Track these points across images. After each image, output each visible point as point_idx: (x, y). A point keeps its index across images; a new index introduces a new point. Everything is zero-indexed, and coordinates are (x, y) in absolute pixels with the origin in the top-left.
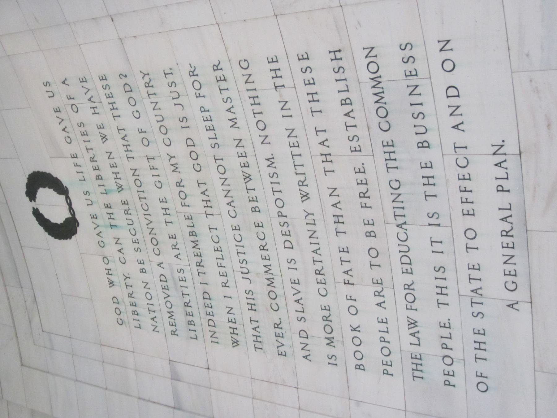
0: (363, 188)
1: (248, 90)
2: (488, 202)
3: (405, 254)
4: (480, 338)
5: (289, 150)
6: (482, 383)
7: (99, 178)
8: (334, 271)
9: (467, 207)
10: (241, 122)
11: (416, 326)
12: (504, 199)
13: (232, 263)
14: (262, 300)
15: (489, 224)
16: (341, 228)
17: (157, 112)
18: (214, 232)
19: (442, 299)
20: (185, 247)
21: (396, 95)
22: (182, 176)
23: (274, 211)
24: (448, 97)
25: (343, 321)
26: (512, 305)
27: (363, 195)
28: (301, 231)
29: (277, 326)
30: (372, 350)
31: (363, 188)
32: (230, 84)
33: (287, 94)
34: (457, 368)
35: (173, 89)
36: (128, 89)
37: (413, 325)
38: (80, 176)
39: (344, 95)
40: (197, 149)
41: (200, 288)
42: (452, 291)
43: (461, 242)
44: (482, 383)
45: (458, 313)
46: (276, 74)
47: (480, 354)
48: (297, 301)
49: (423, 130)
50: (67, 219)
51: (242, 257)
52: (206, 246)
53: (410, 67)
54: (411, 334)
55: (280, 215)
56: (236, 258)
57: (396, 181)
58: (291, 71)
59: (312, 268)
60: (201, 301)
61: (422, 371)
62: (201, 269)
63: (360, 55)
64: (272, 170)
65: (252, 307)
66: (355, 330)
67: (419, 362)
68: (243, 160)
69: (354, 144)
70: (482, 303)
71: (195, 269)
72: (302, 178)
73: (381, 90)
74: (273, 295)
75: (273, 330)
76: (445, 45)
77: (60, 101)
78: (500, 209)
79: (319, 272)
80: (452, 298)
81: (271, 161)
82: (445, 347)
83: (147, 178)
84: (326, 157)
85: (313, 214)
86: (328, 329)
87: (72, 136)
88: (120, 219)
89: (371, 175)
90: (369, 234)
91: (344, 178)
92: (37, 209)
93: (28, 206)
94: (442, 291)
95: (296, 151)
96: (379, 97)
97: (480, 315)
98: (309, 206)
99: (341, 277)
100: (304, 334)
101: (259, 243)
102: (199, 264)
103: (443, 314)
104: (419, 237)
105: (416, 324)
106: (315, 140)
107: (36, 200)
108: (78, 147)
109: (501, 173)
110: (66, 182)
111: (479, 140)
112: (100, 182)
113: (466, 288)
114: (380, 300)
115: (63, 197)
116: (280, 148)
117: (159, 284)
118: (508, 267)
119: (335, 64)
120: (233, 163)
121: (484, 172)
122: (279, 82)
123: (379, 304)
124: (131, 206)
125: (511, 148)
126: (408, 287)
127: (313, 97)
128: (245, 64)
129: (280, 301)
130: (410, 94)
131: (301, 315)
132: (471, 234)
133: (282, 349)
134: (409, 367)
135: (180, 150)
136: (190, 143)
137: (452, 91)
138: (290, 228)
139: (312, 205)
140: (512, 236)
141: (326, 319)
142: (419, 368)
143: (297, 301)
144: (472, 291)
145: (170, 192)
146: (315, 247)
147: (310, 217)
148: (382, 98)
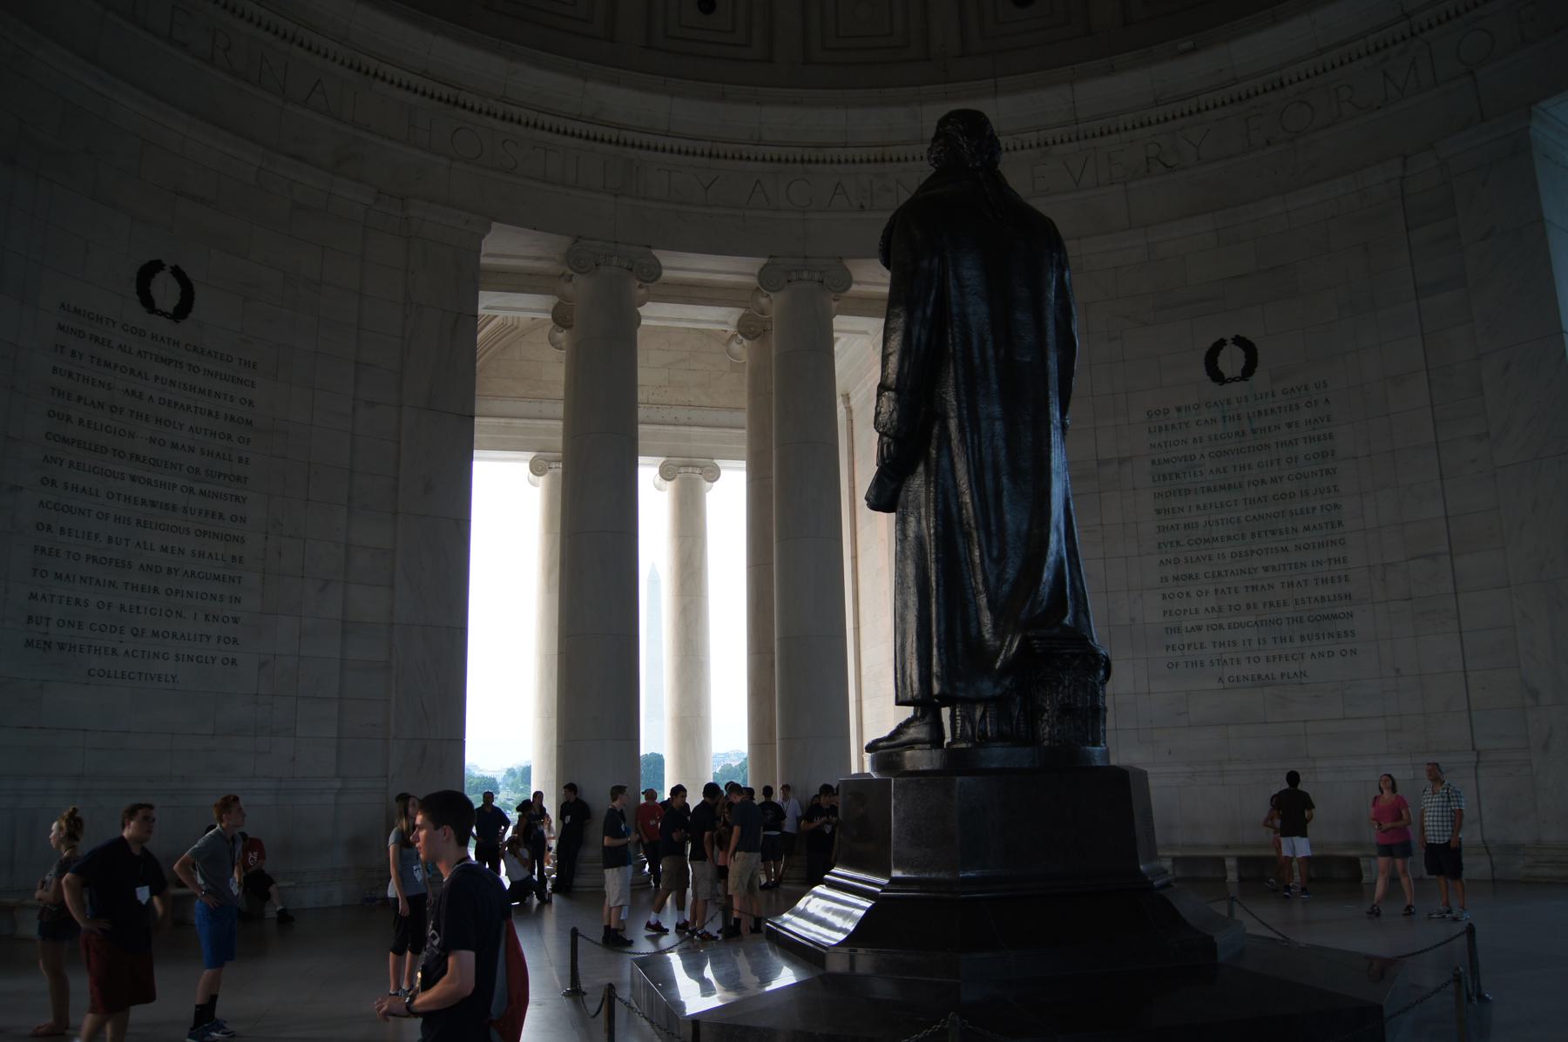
6: (1173, 665)
44: (1173, 665)
46: (1337, 561)
65: (1187, 526)
76: (1354, 652)
81: (1285, 549)
84: (1291, 584)
93: (1229, 336)
94: (1222, 644)
100: (1177, 561)
102: (1209, 489)
110: (1253, 379)
125: (1304, 680)
126: (1221, 626)
127: (1324, 581)
136: (1292, 495)
141: (1190, 577)
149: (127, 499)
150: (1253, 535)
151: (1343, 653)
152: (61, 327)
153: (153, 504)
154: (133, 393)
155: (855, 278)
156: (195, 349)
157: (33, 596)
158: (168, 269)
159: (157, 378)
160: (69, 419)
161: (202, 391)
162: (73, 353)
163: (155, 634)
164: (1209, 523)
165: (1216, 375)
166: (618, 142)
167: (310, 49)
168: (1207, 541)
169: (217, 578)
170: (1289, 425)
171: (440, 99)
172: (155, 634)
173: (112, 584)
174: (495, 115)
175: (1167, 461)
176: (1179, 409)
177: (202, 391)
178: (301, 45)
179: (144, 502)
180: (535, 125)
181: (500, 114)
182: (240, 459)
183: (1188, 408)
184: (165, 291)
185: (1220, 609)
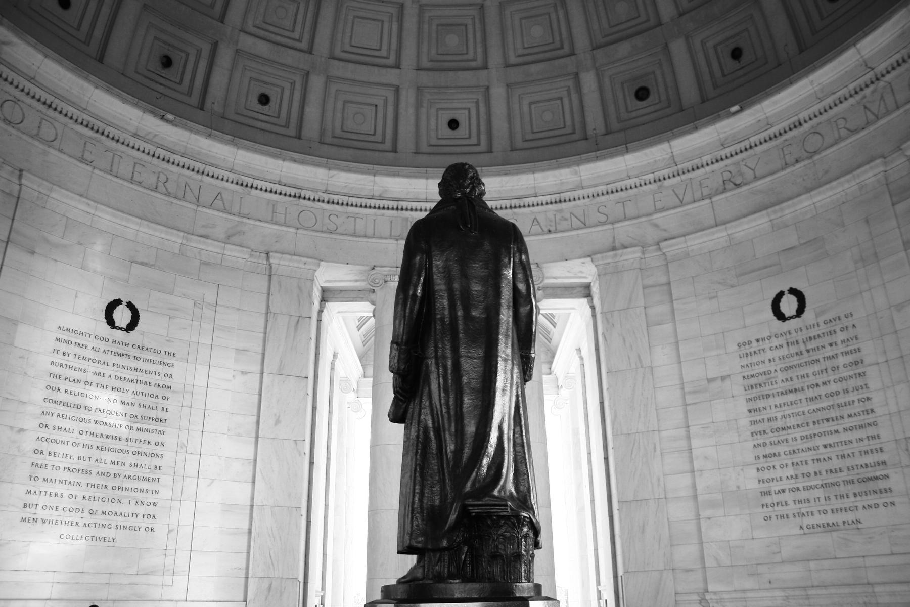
2: (839, 518)
3: (811, 487)
8: (797, 458)
12: (841, 524)
13: (788, 411)
14: (775, 425)
15: (830, 518)
20: (788, 386)
21: (871, 485)
23: (816, 432)
25: (776, 462)
27: (831, 471)
28: (810, 444)
29: (764, 432)
30: (767, 475)
32: (866, 417)
33: (866, 441)
34: (771, 509)
36: (856, 363)
41: (771, 392)
42: (801, 506)
43: (821, 508)
45: (792, 508)
46: (873, 437)
50: (783, 315)
52: (791, 397)
55: (815, 435)
56: (790, 412)
59: (795, 448)
65: (769, 420)
71: (779, 390)
76: (893, 504)
77: (846, 322)
79: (794, 451)
80: (798, 506)
81: (837, 432)
82: (778, 504)
83: (816, 368)
84: (843, 456)
87: (828, 325)
88: (793, 349)
89: (840, 474)
90: (816, 473)
91: (836, 463)
93: (785, 289)
94: (800, 502)
96: (870, 479)
98: (821, 448)
99: (795, 461)
100: (765, 444)
102: (782, 393)
103: (790, 502)
104: (819, 493)
106: (849, 452)
108: (823, 329)
110: (804, 316)
111: (861, 514)
113: (804, 511)
115: (794, 313)
117: (766, 370)
120: (833, 414)
121: (850, 517)
125: (860, 526)
126: (798, 489)
127: (866, 452)
128: (875, 424)
129: (776, 434)
134: (765, 490)
135: (833, 387)
137: (877, 506)
139: (822, 450)
141: (775, 455)
145: (812, 380)
149: (92, 434)
150: (814, 423)
151: (885, 505)
152: (57, 339)
153: (107, 437)
154: (99, 374)
155: (547, 275)
156: (138, 347)
157: (29, 492)
158: (124, 303)
159: (114, 365)
160: (59, 390)
161: (141, 371)
162: (64, 353)
163: (104, 513)
164: (784, 417)
165: (780, 316)
166: (397, 209)
167: (213, 176)
168: (783, 429)
169: (144, 479)
170: (831, 345)
171: (290, 196)
172: (104, 513)
173: (79, 484)
174: (323, 201)
175: (752, 376)
176: (758, 341)
177: (141, 371)
178: (208, 175)
179: (102, 436)
180: (347, 204)
181: (326, 200)
182: (163, 409)
183: (763, 339)
184: (122, 316)
185: (797, 477)
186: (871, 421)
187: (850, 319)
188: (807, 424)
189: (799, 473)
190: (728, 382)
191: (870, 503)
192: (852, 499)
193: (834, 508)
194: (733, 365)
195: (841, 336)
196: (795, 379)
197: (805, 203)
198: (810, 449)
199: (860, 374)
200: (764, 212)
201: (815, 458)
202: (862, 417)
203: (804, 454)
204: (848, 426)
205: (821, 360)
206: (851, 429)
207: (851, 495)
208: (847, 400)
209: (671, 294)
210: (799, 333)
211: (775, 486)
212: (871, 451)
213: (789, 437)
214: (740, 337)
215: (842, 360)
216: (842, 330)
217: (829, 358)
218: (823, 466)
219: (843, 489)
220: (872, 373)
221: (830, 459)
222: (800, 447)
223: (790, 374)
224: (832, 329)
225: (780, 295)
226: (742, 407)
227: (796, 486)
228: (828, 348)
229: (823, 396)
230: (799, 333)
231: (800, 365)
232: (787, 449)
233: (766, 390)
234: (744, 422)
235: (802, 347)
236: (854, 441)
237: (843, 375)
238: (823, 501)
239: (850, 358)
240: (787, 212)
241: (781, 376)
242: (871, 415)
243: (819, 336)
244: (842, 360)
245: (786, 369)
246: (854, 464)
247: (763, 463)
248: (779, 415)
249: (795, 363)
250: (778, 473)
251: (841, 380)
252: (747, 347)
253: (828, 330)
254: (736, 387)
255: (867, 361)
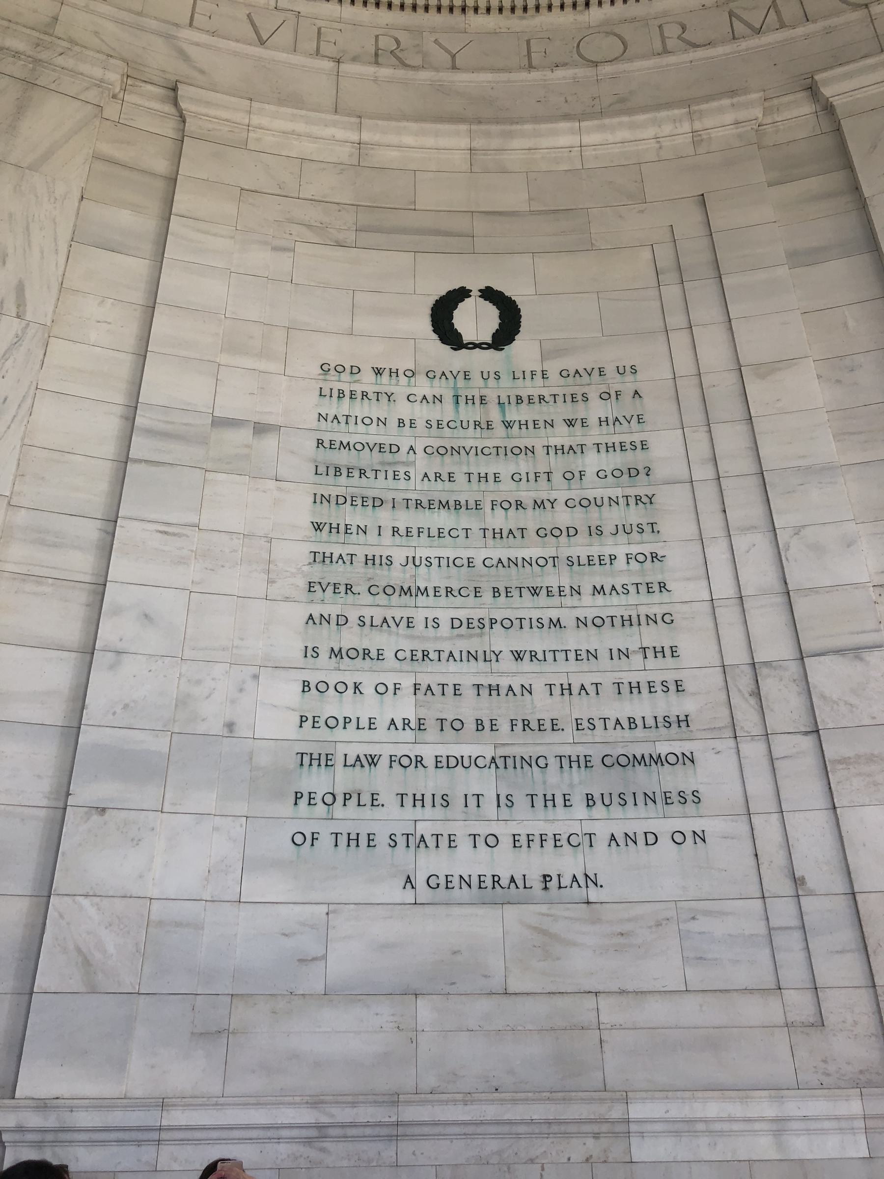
0: (534, 725)
1: (638, 616)
2: (533, 864)
3: (459, 761)
4: (363, 841)
5: (573, 648)
7: (519, 399)
9: (523, 841)
10: (600, 600)
11: (370, 765)
14: (383, 577)
15: (505, 862)
16: (484, 692)
17: (606, 500)
18: (463, 534)
19: (408, 801)
20: (440, 490)
21: (644, 779)
22: (530, 511)
23: (498, 615)
24: (645, 833)
26: (410, 882)
27: (526, 724)
28: (474, 644)
29: (349, 588)
31: (534, 725)
32: (644, 598)
33: (637, 660)
35: (635, 528)
36: (632, 473)
37: (370, 761)
38: (519, 374)
39: (639, 722)
40: (563, 539)
41: (388, 496)
43: (483, 829)
45: (391, 818)
46: (660, 652)
47: (343, 840)
48: (385, 620)
49: (607, 802)
50: (460, 335)
51: (435, 562)
52: (442, 519)
53: (675, 798)
54: (358, 756)
55: (493, 622)
56: (433, 553)
57: (547, 764)
58: (658, 670)
59: (431, 647)
60: (371, 493)
61: (311, 765)
62: (412, 504)
63: (685, 747)
64: (546, 622)
65: (369, 560)
66: (356, 687)
67: (323, 762)
68: (555, 590)
69: (585, 724)
70: (408, 846)
71: (414, 496)
72: (540, 656)
73: (648, 764)
74: (389, 591)
75: (344, 581)
77: (615, 383)
78: (524, 876)
79: (425, 655)
80: (410, 812)
81: (556, 624)
82: (347, 797)
83: (523, 465)
85: (497, 661)
86: (353, 654)
89: (550, 737)
90: (479, 723)
91: (543, 705)
92: (470, 296)
93: (475, 285)
94: (418, 800)
95: (571, 656)
96: (640, 760)
97: (393, 844)
98: (506, 656)
99: (424, 680)
100: (342, 621)
101: (456, 587)
102: (418, 504)
103: (388, 797)
104: (483, 783)
105: (373, 765)
106: (588, 680)
107: (482, 299)
108: (556, 384)
109: (566, 881)
111: (600, 860)
112: (513, 400)
113: (423, 829)
114: (400, 725)
115: (489, 340)
116: (574, 639)
117: (386, 440)
118: (456, 881)
119: (673, 719)
120: (551, 579)
122: (650, 654)
123: (393, 722)
124: (486, 433)
125: (594, 894)
126: (419, 761)
127: (635, 688)
128: (667, 619)
129: (382, 599)
130: (645, 794)
131: (368, 621)
132: (492, 841)
133: (317, 587)
134: (315, 749)
135: (563, 517)
136: (572, 532)
137: (652, 839)
138: (478, 631)
139: (507, 663)
140: (494, 888)
141: (366, 653)
142: (315, 763)
143: (385, 620)
144: (422, 836)
145: (507, 490)
146: (457, 655)
147: (494, 657)
148: (640, 764)
151: (678, 838)
168: (406, 591)
170: (570, 423)
176: (378, 372)
183: (394, 373)
185: (421, 725)
186: (658, 610)
187: (629, 377)
188: (477, 591)
189: (431, 716)
190: (270, 442)
191: (632, 827)
192: (580, 810)
193: (522, 830)
194: (298, 404)
195: (597, 409)
196: (460, 478)
197: (563, 137)
198: (472, 656)
199: (638, 499)
200: (463, 127)
201: (485, 681)
202: (633, 598)
203: (452, 666)
204: (590, 614)
205: (540, 452)
206: (598, 623)
207: (578, 801)
208: (595, 551)
209: (169, 202)
210: (492, 382)
211: (350, 743)
212: (650, 685)
213: (419, 616)
214: (332, 350)
215: (592, 462)
216: (605, 396)
217: (560, 450)
218: (503, 710)
219: (554, 780)
220: (673, 501)
221: (528, 690)
222: (447, 647)
223: (448, 464)
224: (579, 391)
225: (462, 294)
226: (299, 510)
227: (414, 751)
228: (563, 429)
229: (531, 533)
230: (492, 382)
231: (481, 452)
232: (407, 645)
233: (378, 486)
234: (294, 554)
235: (495, 415)
236: (604, 654)
237: (590, 494)
238: (489, 807)
239: (616, 460)
240: (516, 143)
241: (422, 464)
242: (656, 597)
243: (541, 398)
244: (592, 462)
245: (441, 452)
246: (596, 714)
247: (325, 671)
248: (399, 556)
249: (468, 444)
250: (367, 707)
251: (585, 504)
252: (345, 376)
253: (569, 391)
254: (295, 456)
255: (660, 472)
